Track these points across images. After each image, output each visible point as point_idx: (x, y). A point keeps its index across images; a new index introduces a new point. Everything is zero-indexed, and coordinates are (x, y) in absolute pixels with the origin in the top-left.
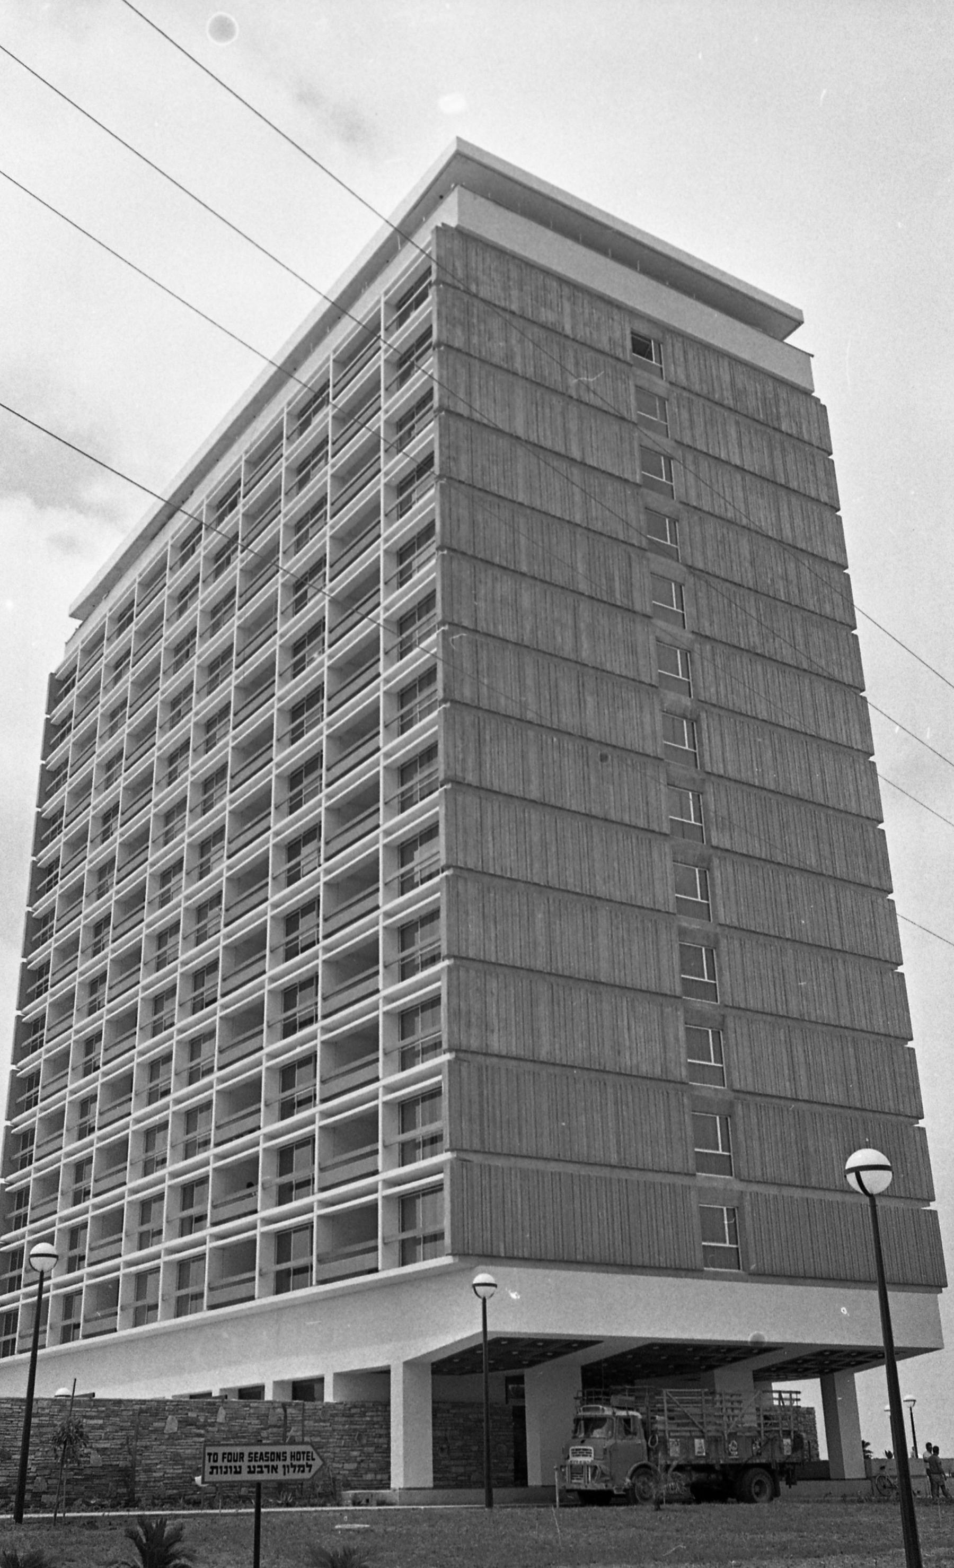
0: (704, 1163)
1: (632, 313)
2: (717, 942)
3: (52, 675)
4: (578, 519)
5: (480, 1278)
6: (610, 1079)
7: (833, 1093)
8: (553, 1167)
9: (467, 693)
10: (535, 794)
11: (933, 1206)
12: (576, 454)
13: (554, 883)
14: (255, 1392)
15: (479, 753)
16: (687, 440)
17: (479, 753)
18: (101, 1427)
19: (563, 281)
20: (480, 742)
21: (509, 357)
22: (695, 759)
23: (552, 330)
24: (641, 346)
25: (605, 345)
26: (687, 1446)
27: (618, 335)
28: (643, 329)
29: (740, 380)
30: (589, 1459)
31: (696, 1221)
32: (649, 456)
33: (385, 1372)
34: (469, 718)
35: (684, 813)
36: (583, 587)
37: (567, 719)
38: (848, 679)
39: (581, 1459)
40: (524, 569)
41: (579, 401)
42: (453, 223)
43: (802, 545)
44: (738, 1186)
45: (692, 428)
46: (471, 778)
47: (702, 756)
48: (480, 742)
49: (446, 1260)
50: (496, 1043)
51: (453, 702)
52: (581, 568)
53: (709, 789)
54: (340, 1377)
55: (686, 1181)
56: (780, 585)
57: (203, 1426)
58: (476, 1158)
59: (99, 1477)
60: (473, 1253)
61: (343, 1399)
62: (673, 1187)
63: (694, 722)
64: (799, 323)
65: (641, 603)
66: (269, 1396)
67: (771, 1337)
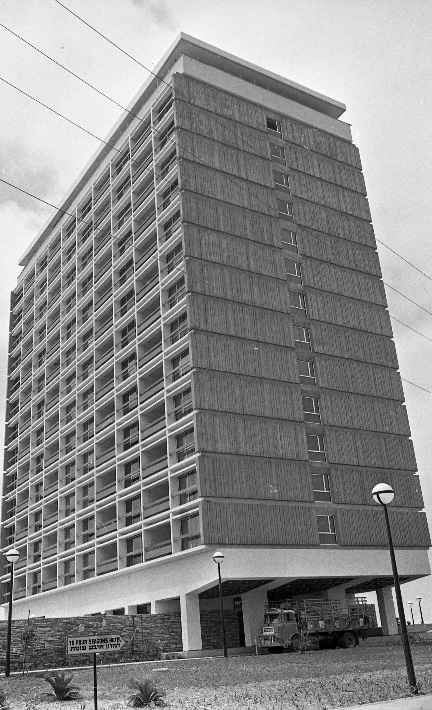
0: (318, 496)
1: (267, 109)
2: (319, 396)
4: (246, 206)
5: (217, 554)
6: (273, 461)
8: (248, 502)
9: (199, 288)
10: (232, 332)
11: (423, 510)
12: (244, 176)
13: (243, 372)
14: (121, 611)
15: (206, 315)
16: (295, 167)
17: (206, 315)
18: (49, 631)
19: (234, 96)
20: (206, 310)
22: (305, 313)
23: (230, 119)
24: (271, 124)
25: (254, 125)
26: (316, 624)
27: (261, 120)
28: (272, 116)
30: (271, 633)
31: (315, 522)
32: (278, 176)
33: (178, 599)
34: (200, 299)
35: (301, 338)
36: (250, 236)
37: (246, 298)
38: (374, 272)
39: (268, 633)
40: (222, 230)
41: (244, 151)
42: (181, 72)
44: (334, 506)
45: (297, 161)
46: (203, 327)
47: (308, 311)
48: (206, 310)
49: (203, 547)
50: (220, 447)
51: (192, 292)
52: (248, 227)
53: (312, 326)
54: (158, 602)
55: (310, 505)
56: (341, 231)
57: (96, 628)
58: (214, 500)
59: (50, 654)
60: (213, 543)
61: (161, 612)
62: (304, 508)
63: (304, 296)
64: (344, 110)
66: (126, 612)
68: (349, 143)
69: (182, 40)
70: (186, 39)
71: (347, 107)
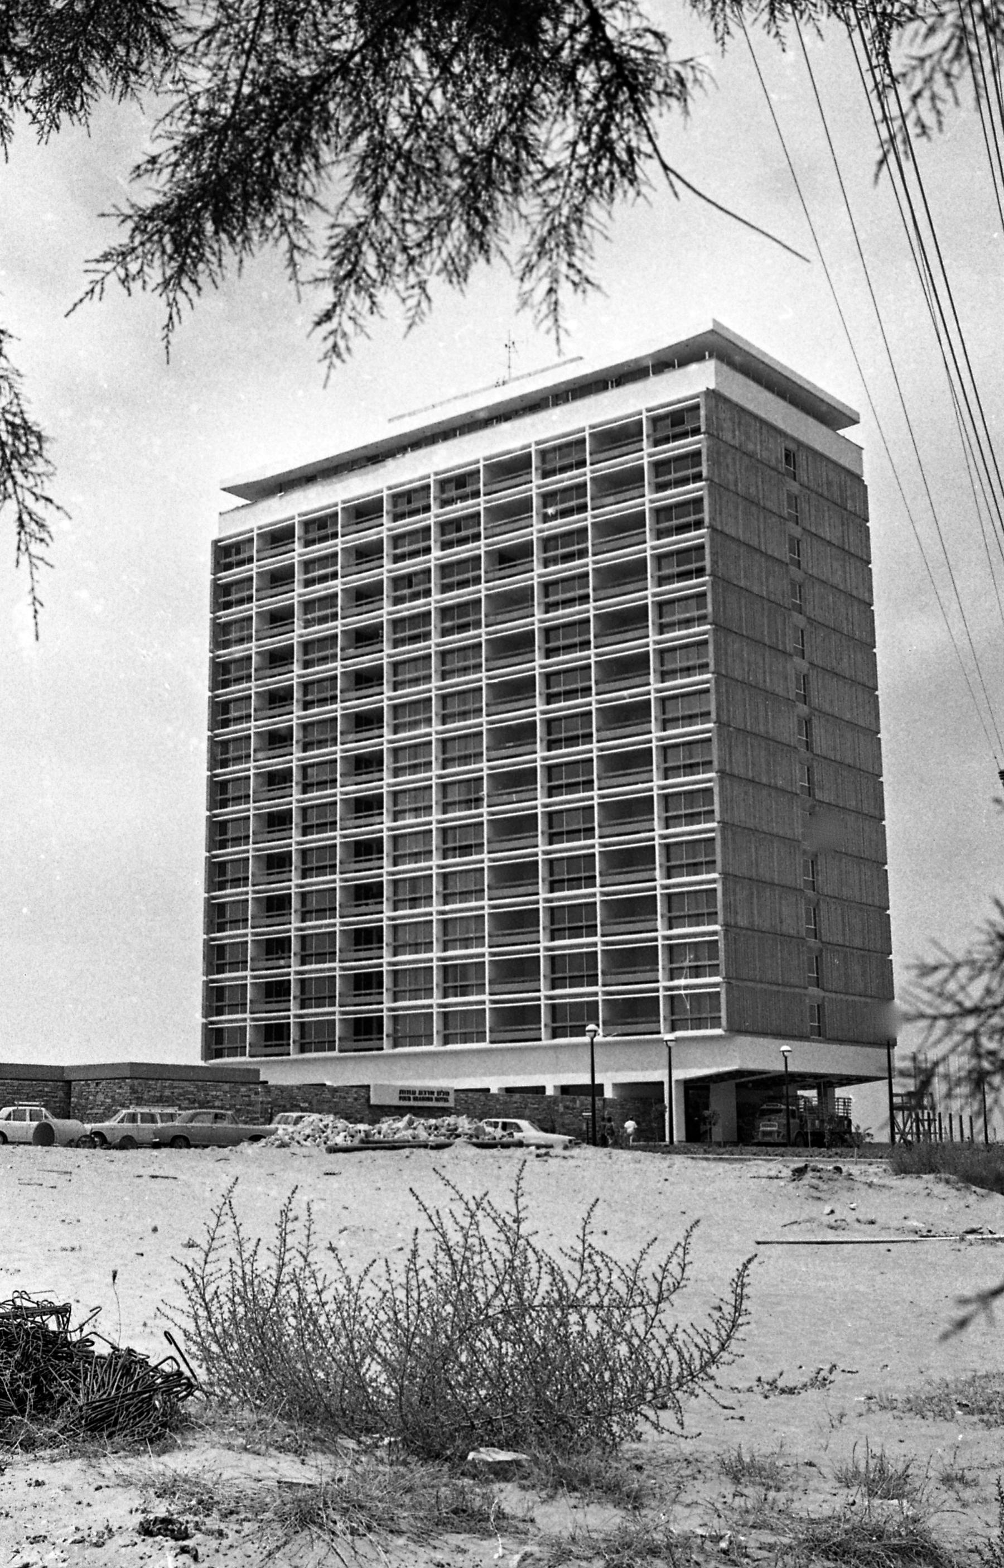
3: (215, 543)
5: (784, 1048)
7: (858, 942)
8: (759, 986)
9: (724, 719)
12: (763, 549)
19: (756, 417)
20: (730, 747)
21: (736, 485)
23: (751, 455)
25: (773, 463)
29: (832, 475)
32: (795, 545)
36: (767, 641)
42: (712, 386)
43: (855, 593)
44: (822, 994)
48: (730, 747)
55: (803, 991)
60: (735, 1029)
63: (808, 722)
64: (856, 422)
65: (789, 648)
66: (609, 1093)
67: (751, 1066)
68: (858, 478)
69: (712, 332)
70: (721, 332)
71: (862, 420)
